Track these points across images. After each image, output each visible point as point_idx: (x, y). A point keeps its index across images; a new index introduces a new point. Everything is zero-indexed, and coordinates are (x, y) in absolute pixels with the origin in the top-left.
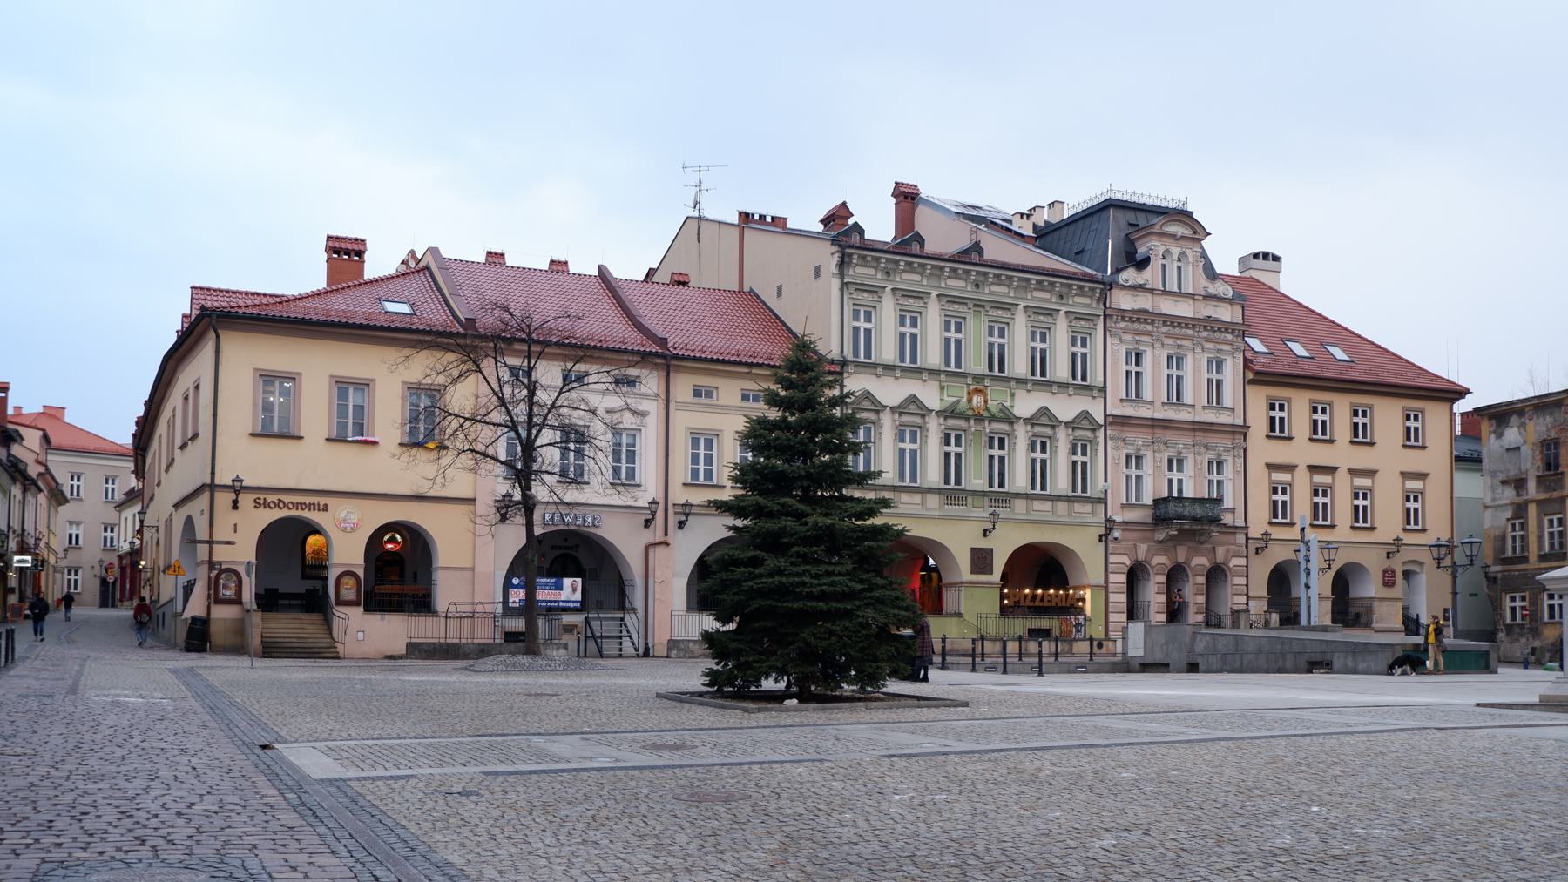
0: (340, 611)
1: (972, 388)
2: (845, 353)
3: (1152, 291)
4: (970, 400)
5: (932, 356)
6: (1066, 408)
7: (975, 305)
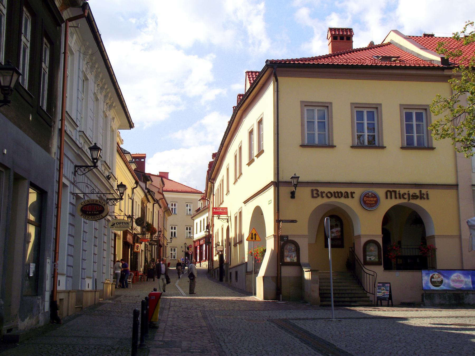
0: (369, 269)
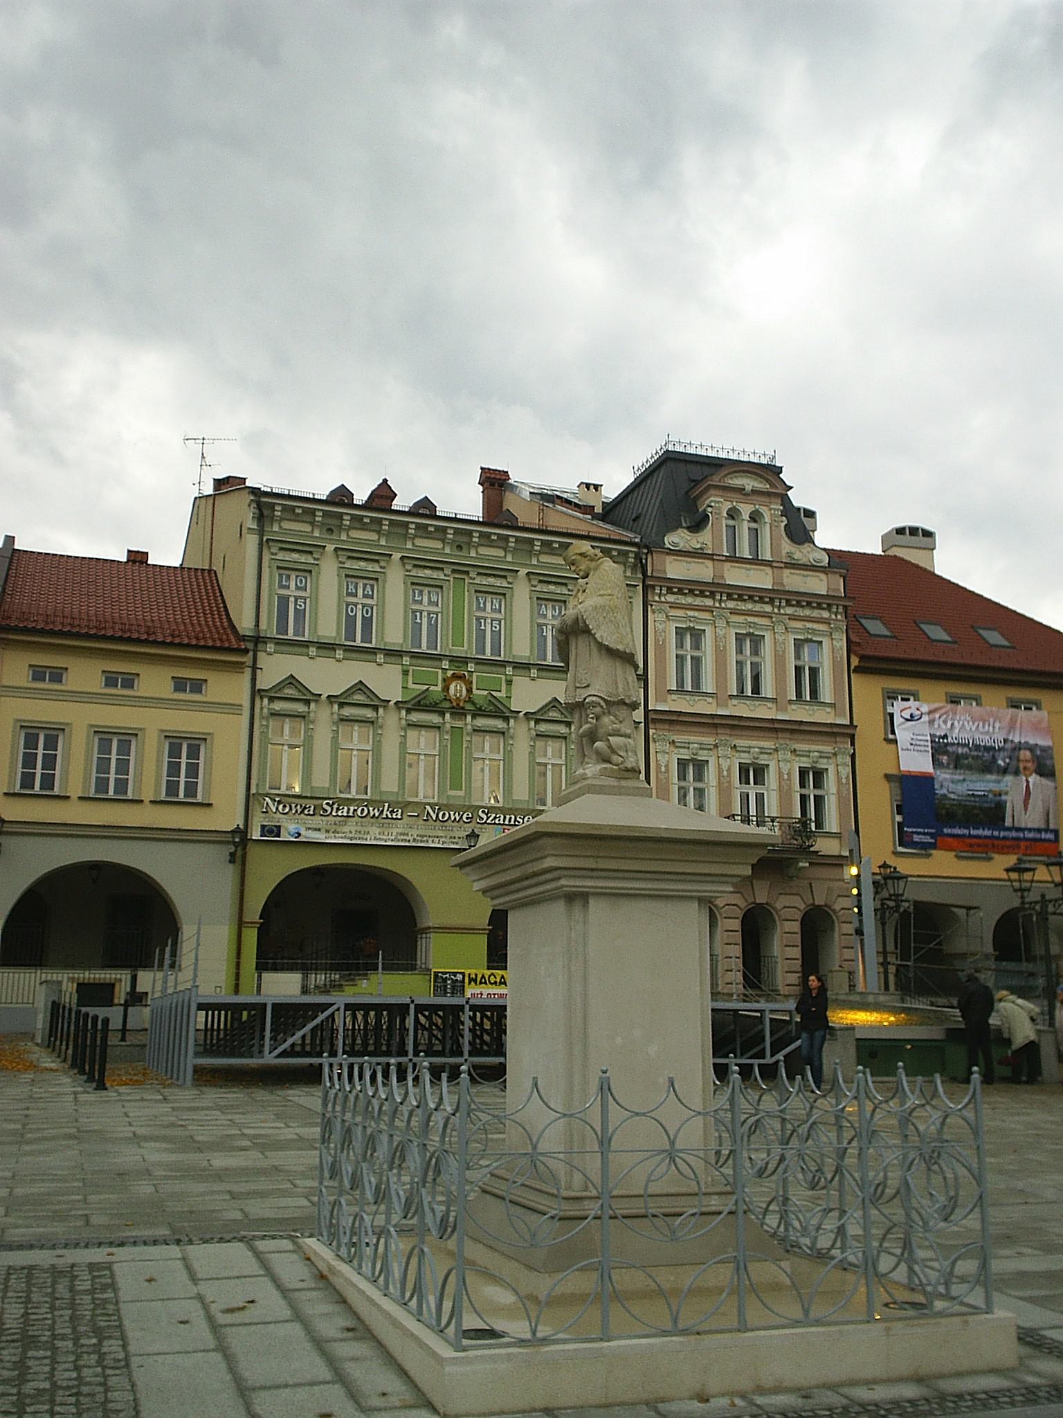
1: (450, 673)
2: (263, 625)
3: (710, 557)
4: (446, 689)
7: (454, 571)
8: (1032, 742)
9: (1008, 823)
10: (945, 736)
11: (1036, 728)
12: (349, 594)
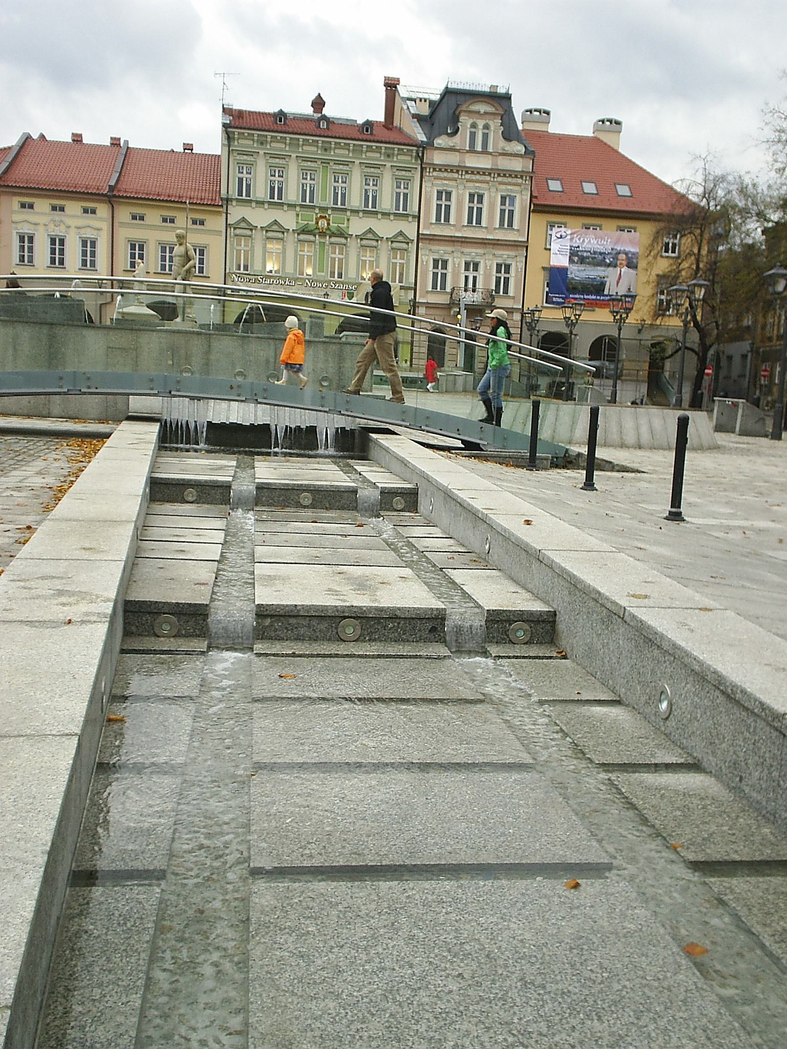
3: (458, 151)
4: (317, 223)
5: (292, 194)
6: (386, 228)
8: (627, 250)
9: (606, 292)
10: (579, 247)
11: (632, 242)
12: (271, 176)
